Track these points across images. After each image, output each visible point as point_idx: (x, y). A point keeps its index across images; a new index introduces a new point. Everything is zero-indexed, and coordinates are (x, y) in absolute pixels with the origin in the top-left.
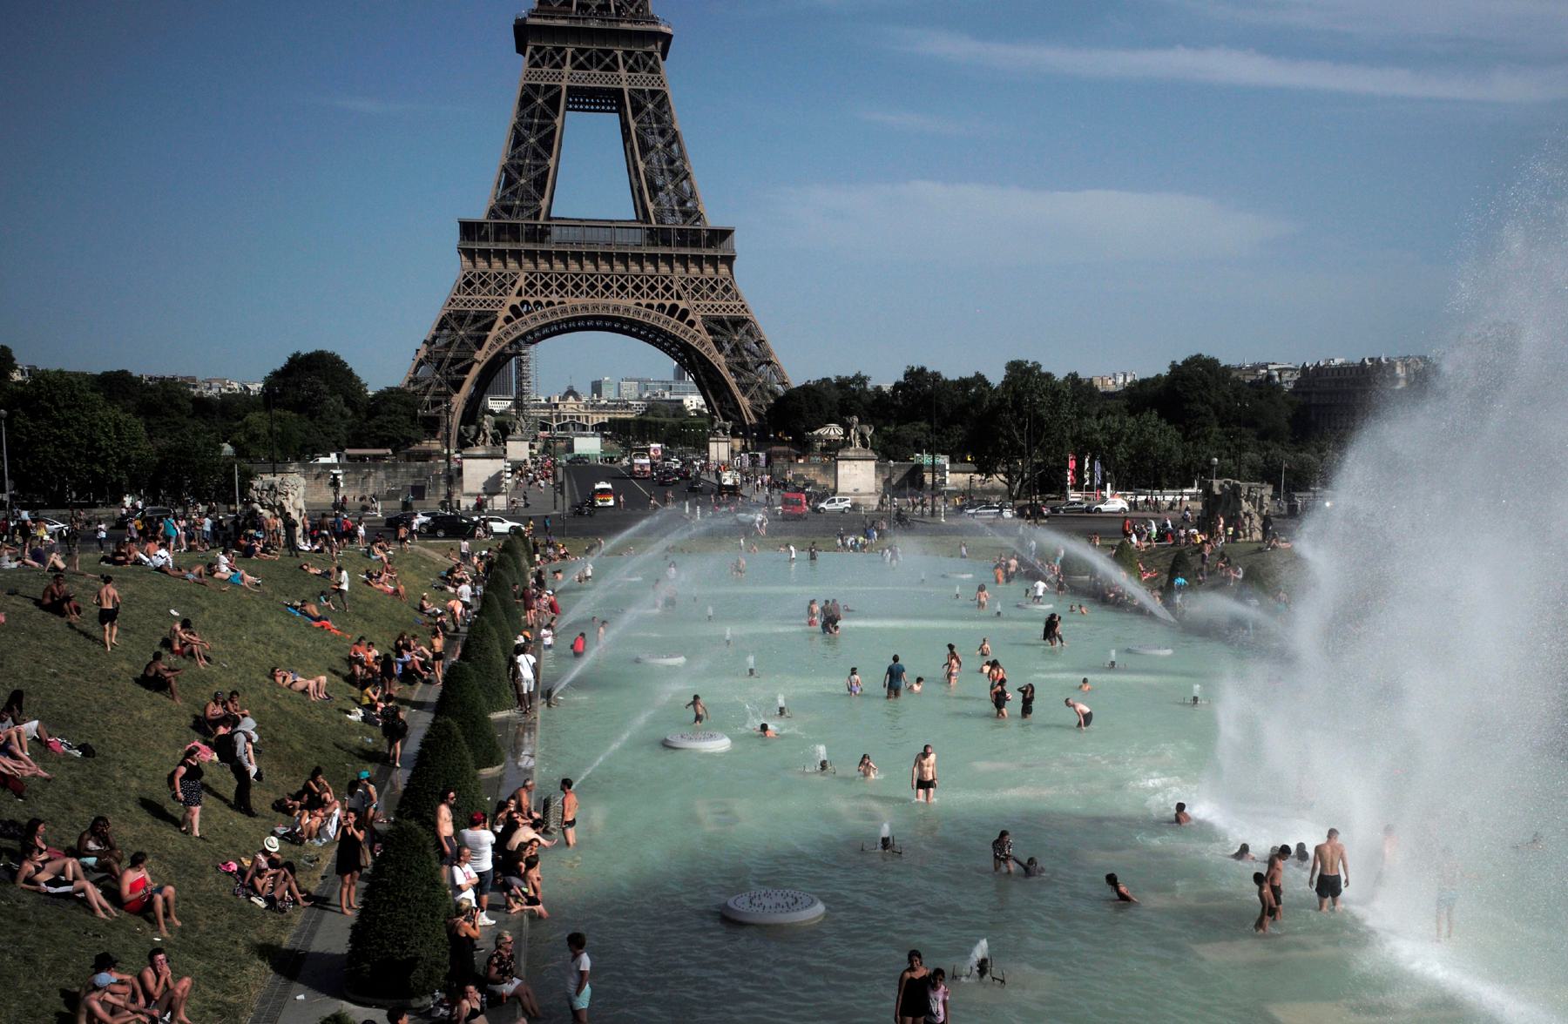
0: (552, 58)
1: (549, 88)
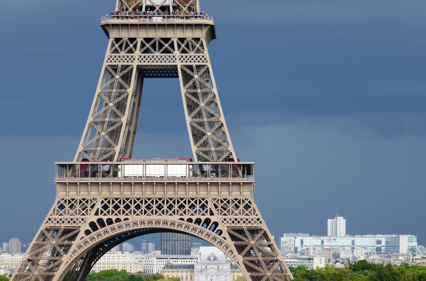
0: (127, 45)
1: (124, 67)
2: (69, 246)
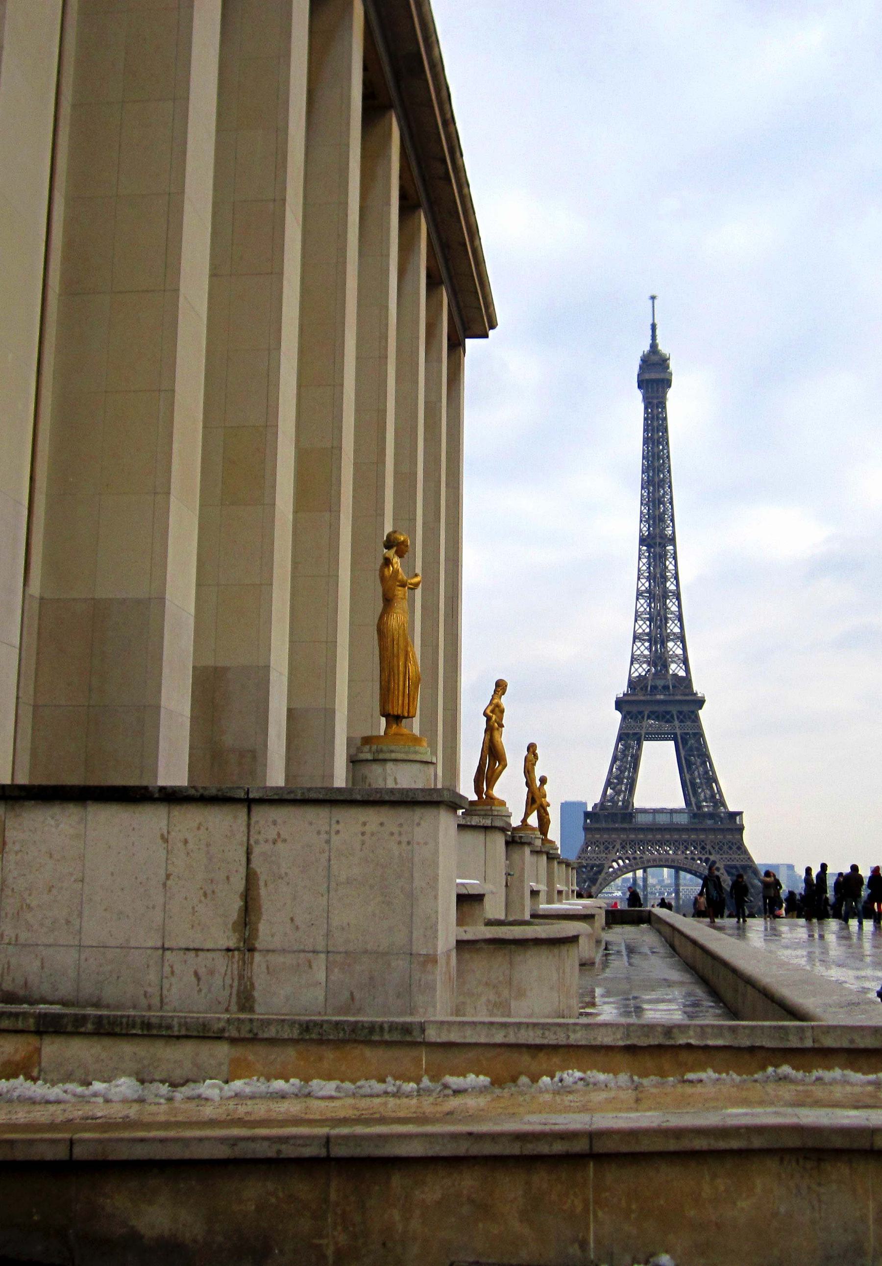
0: (637, 717)
2: (597, 880)
